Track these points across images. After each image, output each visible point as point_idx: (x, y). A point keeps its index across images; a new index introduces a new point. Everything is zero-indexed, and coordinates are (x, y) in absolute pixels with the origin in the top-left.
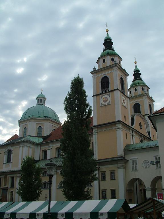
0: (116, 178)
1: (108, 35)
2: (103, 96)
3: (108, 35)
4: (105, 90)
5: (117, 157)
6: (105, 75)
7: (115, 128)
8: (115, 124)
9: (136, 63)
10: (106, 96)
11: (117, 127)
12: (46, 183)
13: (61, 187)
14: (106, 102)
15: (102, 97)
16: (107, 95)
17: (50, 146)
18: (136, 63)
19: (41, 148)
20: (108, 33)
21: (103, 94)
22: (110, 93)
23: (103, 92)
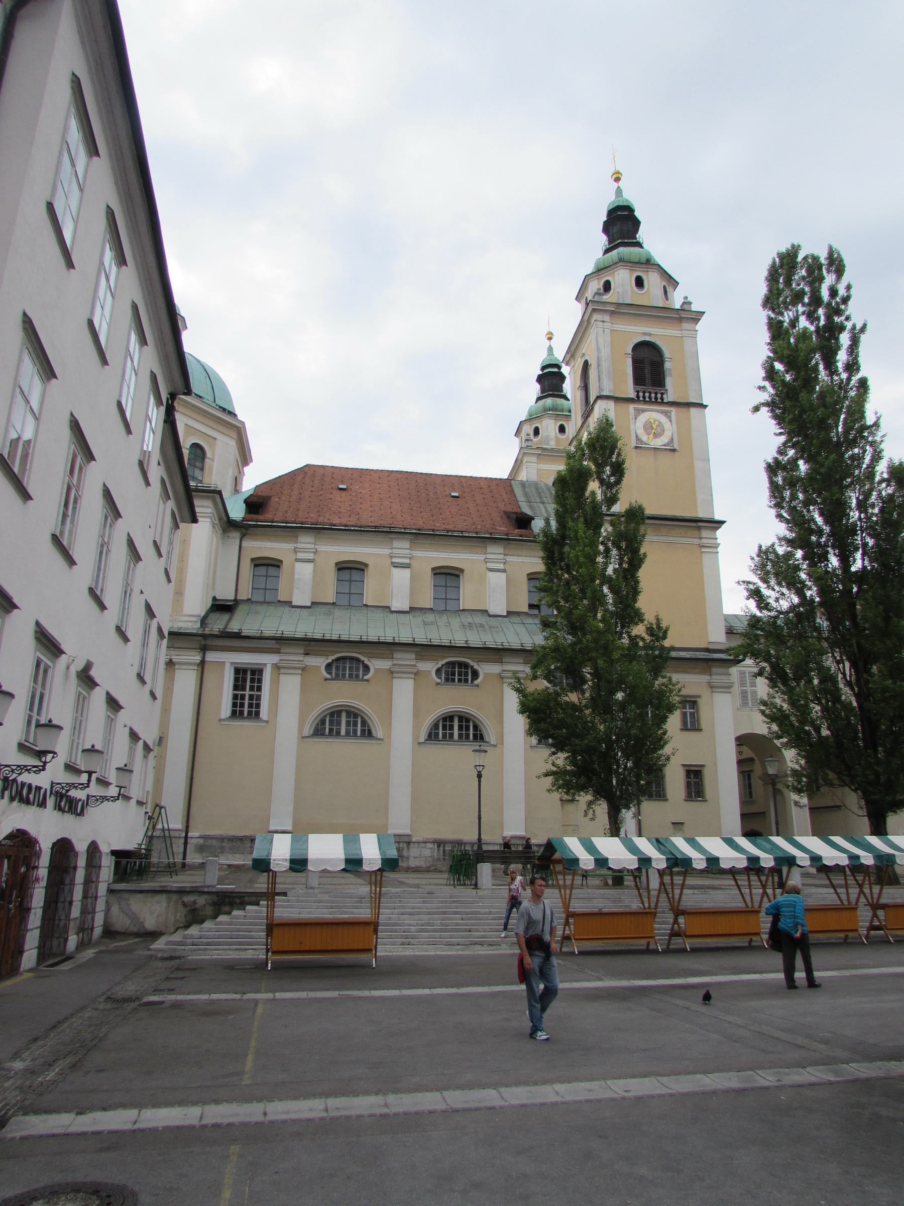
0: (704, 724)
1: (619, 192)
2: (643, 411)
3: (619, 192)
4: (650, 393)
5: (707, 650)
6: (650, 335)
7: (697, 541)
8: (699, 528)
9: (550, 339)
10: (652, 415)
11: (704, 541)
12: (339, 713)
13: (531, 735)
14: (656, 436)
15: (638, 412)
16: (662, 412)
17: (299, 545)
18: (550, 339)
19: (245, 544)
20: (621, 184)
21: (645, 402)
22: (673, 411)
23: (638, 396)
